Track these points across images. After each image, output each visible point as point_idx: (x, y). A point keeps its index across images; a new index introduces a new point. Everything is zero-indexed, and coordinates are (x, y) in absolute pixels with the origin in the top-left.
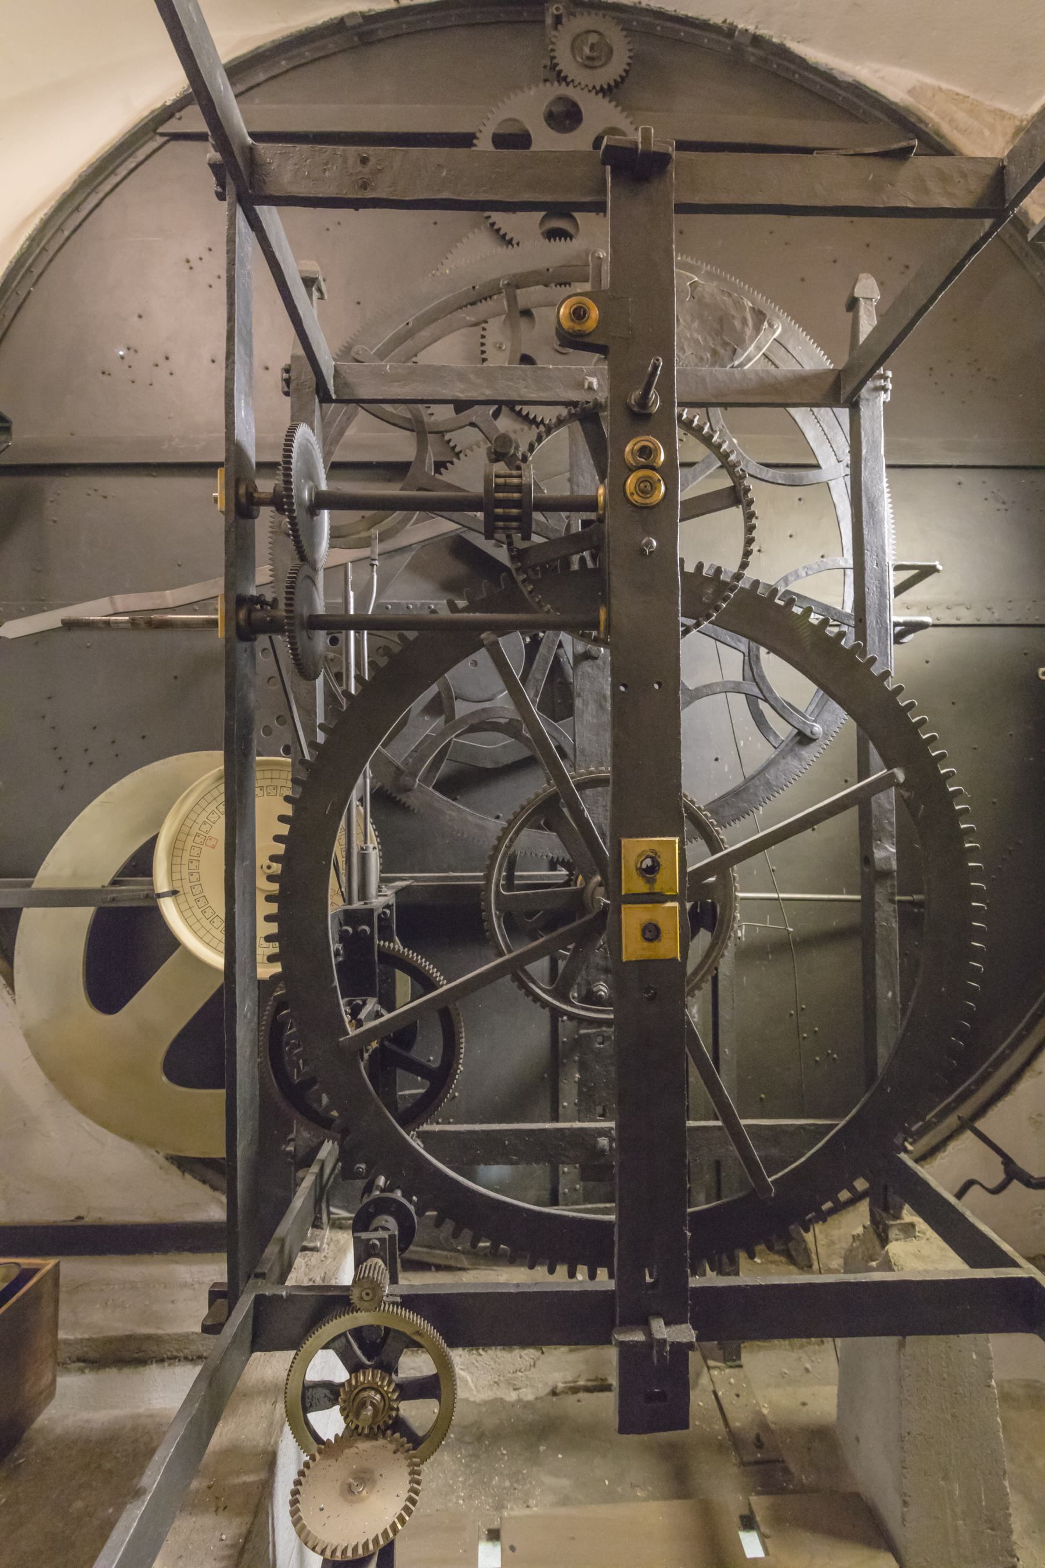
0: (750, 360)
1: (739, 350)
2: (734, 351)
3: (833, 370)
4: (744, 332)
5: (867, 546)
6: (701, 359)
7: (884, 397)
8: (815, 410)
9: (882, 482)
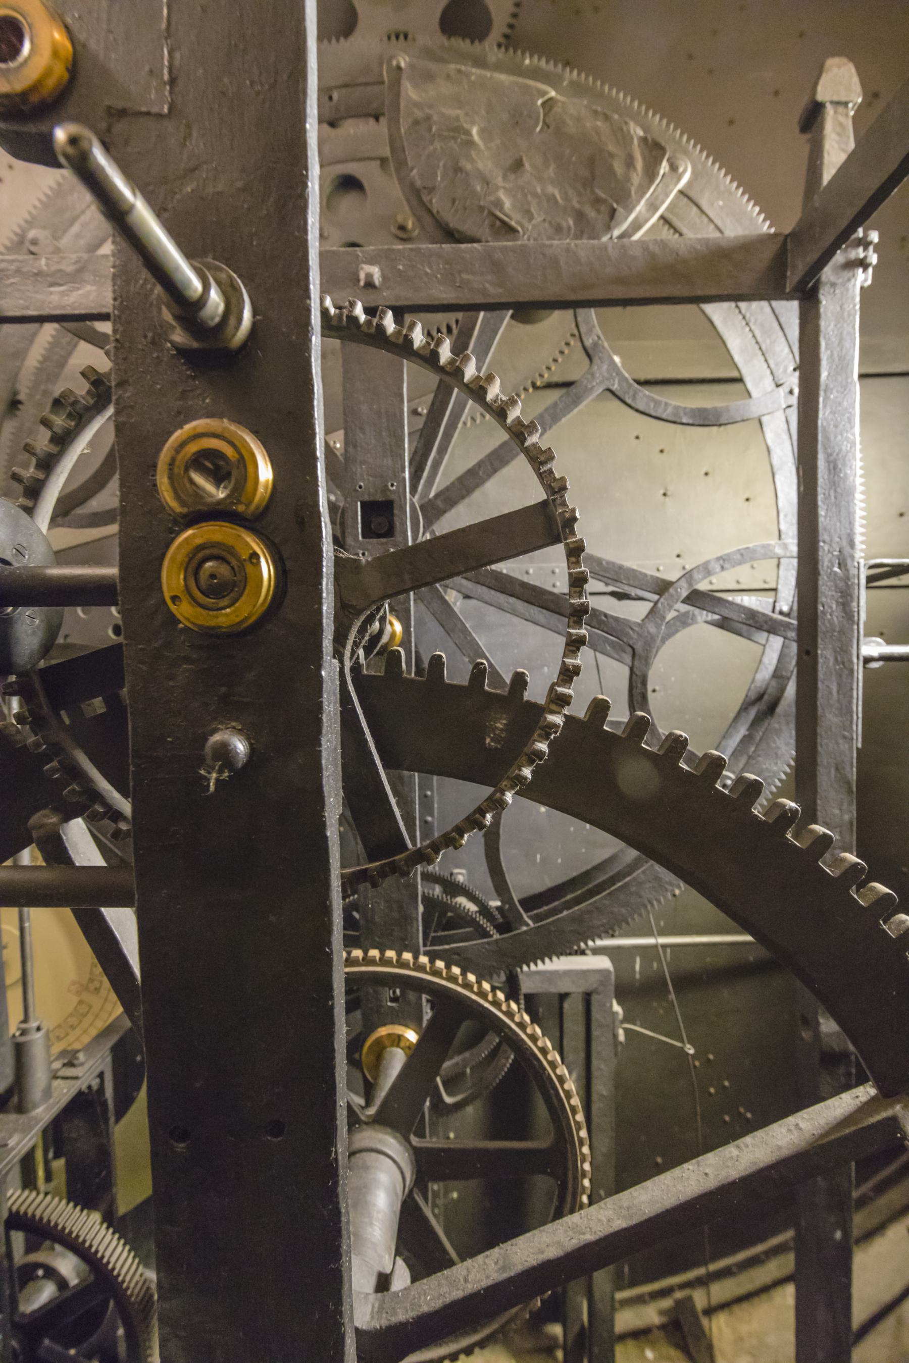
0: (639, 227)
1: (620, 210)
2: (613, 212)
3: (775, 235)
4: (628, 179)
5: (823, 535)
6: (558, 229)
7: (863, 278)
8: (743, 305)
9: (852, 427)
